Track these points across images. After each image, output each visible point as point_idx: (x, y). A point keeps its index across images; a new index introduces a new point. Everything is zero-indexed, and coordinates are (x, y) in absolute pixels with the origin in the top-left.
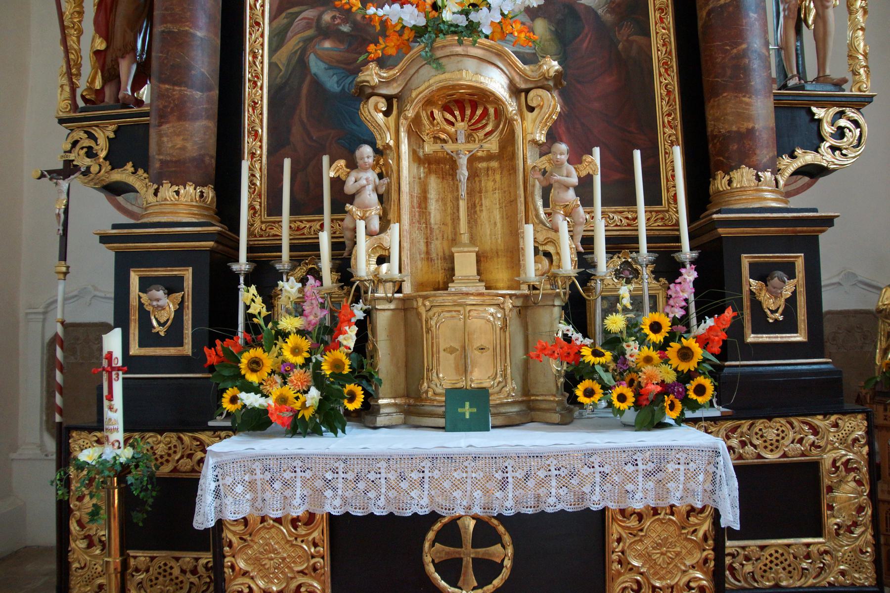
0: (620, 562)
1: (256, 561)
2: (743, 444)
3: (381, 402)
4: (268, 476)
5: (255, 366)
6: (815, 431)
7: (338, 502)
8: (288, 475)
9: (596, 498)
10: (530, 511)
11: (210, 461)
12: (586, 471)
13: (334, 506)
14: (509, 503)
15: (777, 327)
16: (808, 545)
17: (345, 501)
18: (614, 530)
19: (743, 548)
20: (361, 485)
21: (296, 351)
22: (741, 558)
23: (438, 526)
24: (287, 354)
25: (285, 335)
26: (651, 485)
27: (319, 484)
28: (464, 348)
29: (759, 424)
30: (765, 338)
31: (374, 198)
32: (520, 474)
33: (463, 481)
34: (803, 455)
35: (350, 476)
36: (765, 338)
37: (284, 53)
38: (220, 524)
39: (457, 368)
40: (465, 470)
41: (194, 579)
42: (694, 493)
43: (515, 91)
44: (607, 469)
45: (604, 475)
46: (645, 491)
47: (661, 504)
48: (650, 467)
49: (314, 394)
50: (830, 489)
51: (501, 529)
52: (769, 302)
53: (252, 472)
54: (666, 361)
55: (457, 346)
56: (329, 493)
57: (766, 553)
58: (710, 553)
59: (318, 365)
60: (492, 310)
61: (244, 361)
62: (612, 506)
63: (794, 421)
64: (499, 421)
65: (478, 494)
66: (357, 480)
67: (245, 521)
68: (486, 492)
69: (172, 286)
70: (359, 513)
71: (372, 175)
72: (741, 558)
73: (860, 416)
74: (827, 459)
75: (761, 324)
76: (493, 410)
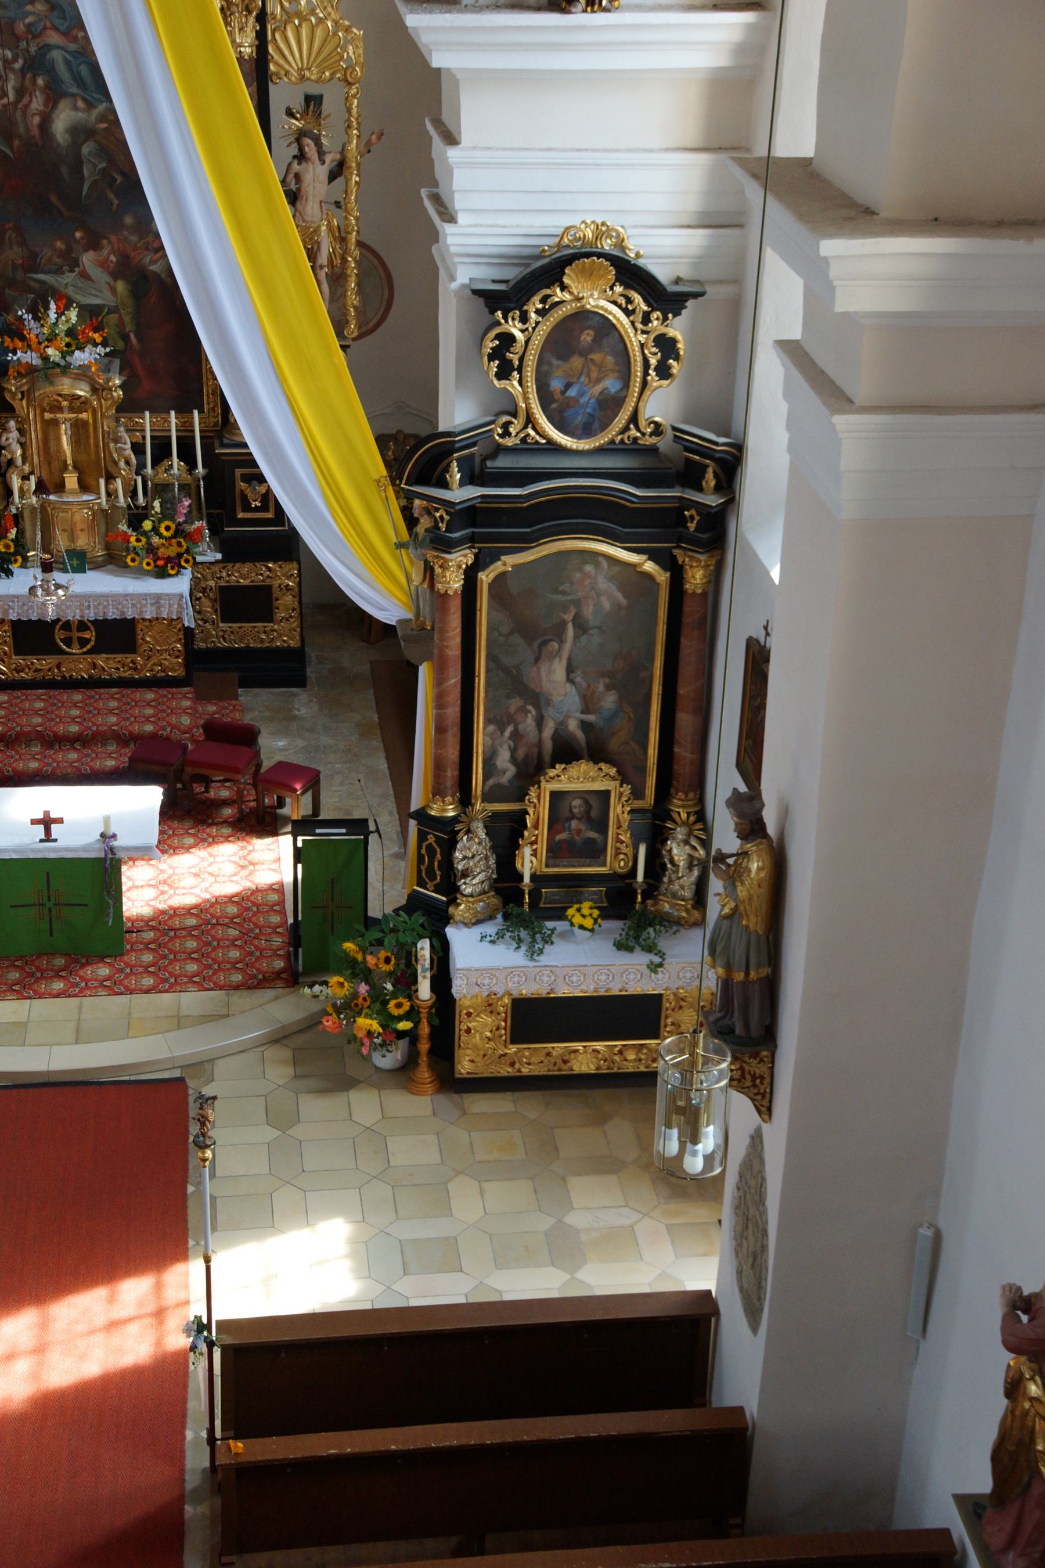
0: (142, 639)
2: (229, 575)
3: (29, 554)
6: (269, 569)
7: (15, 615)
9: (129, 614)
10: (101, 618)
12: (125, 602)
13: (13, 616)
14: (92, 615)
15: (257, 509)
16: (265, 627)
17: (18, 614)
18: (140, 626)
19: (230, 627)
20: (25, 608)
22: (228, 633)
23: (61, 623)
26: (154, 608)
27: (6, 607)
28: (72, 530)
29: (238, 565)
30: (249, 515)
31: (19, 445)
32: (96, 603)
33: (71, 606)
34: (263, 581)
35: (20, 604)
36: (249, 515)
39: (69, 539)
40: (72, 601)
42: (172, 612)
43: (95, 390)
44: (134, 602)
45: (133, 604)
46: (151, 611)
47: (159, 616)
48: (153, 601)
50: (277, 599)
51: (90, 624)
52: (250, 496)
54: (170, 545)
55: (68, 528)
56: (11, 611)
57: (243, 629)
58: (182, 637)
60: (86, 511)
62: (137, 617)
63: (257, 564)
64: (92, 566)
65: (78, 611)
66: (24, 605)
68: (82, 611)
70: (25, 619)
71: (14, 435)
72: (228, 633)
73: (295, 563)
74: (276, 583)
75: (246, 507)
76: (88, 560)
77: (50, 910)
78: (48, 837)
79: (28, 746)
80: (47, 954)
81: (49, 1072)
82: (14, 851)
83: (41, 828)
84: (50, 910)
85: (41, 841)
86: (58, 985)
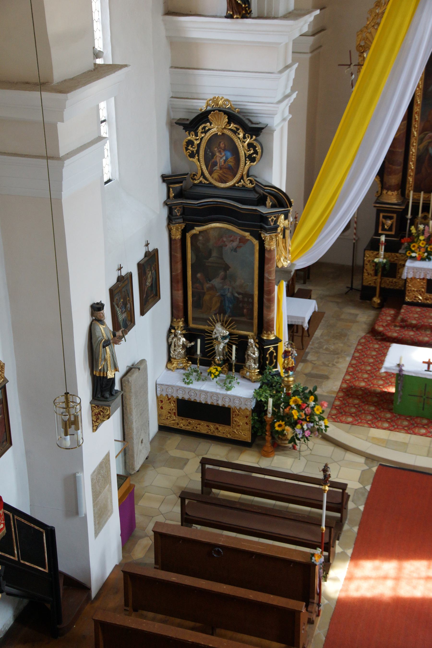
1: (412, 285)
4: (417, 271)
5: (414, 246)
7: (429, 277)
8: (421, 271)
11: (406, 268)
21: (423, 244)
24: (421, 244)
25: (421, 240)
27: (426, 273)
37: (422, 146)
38: (407, 278)
41: (391, 284)
49: (426, 254)
53: (414, 270)
56: (428, 275)
59: (427, 248)
61: (412, 245)
67: (411, 278)
69: (391, 218)
77: (424, 399)
78: (428, 370)
79: (425, 331)
80: (421, 417)
81: (414, 466)
82: (414, 373)
83: (426, 365)
84: (424, 399)
85: (426, 371)
86: (423, 431)
